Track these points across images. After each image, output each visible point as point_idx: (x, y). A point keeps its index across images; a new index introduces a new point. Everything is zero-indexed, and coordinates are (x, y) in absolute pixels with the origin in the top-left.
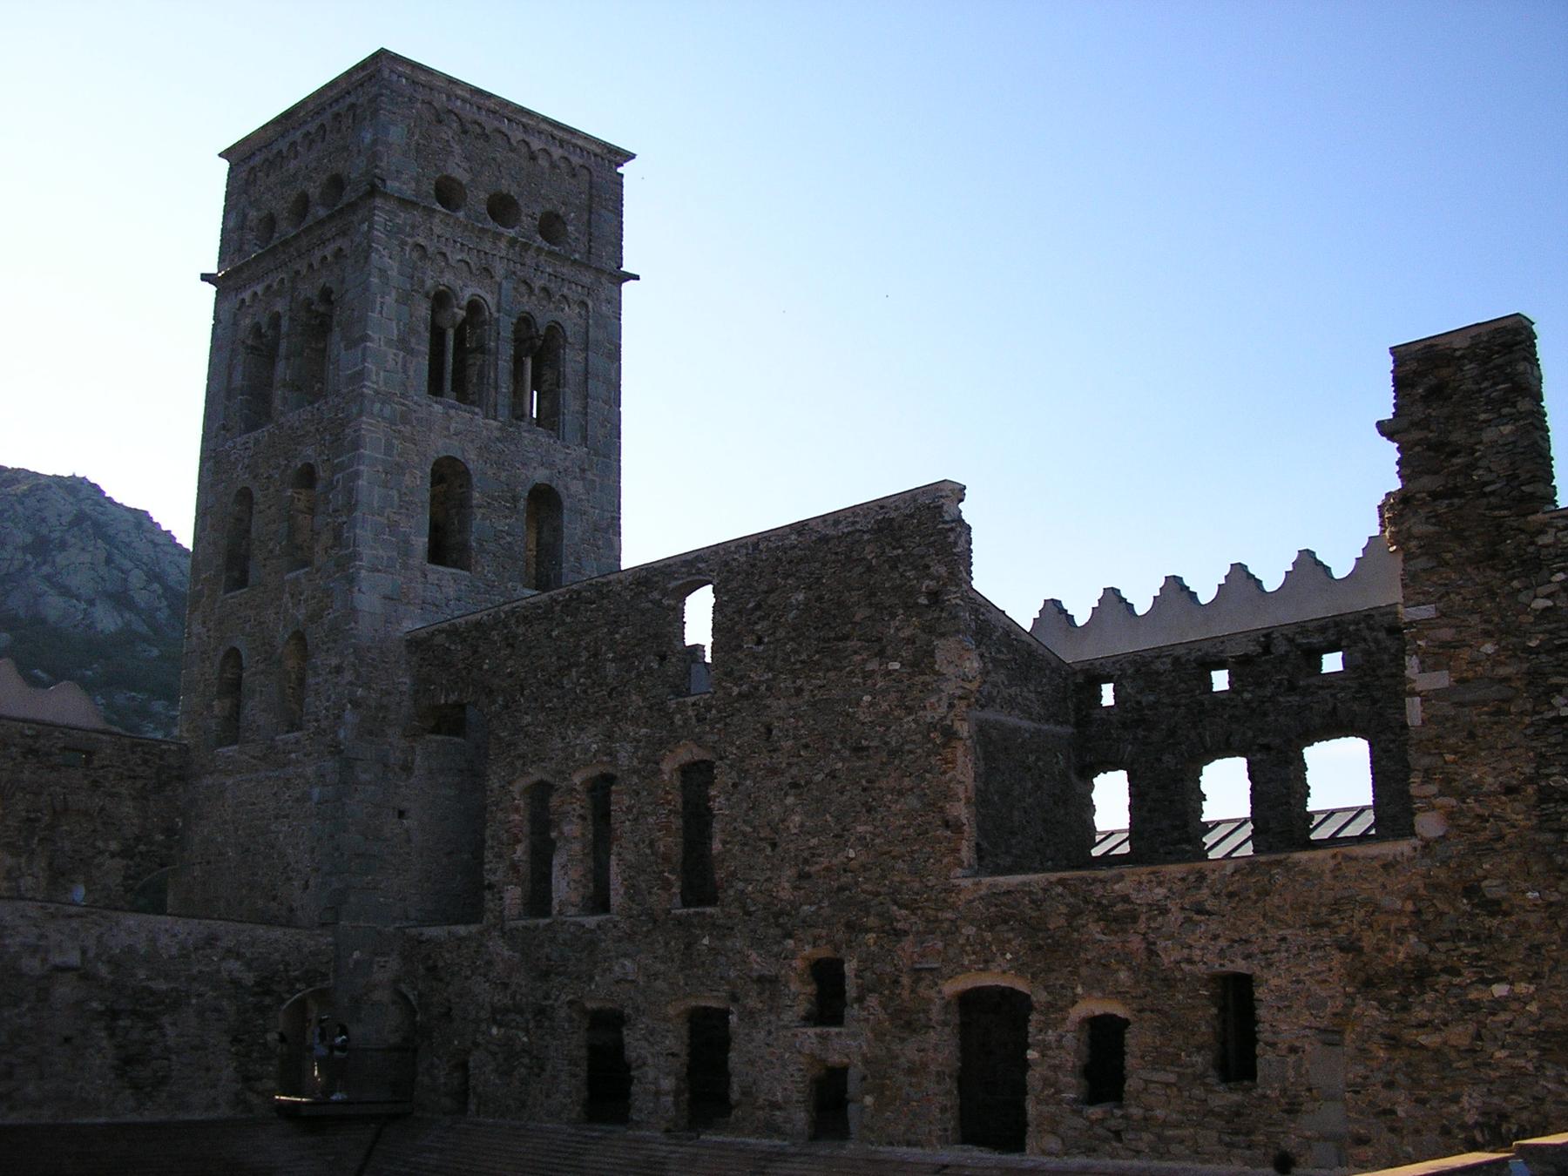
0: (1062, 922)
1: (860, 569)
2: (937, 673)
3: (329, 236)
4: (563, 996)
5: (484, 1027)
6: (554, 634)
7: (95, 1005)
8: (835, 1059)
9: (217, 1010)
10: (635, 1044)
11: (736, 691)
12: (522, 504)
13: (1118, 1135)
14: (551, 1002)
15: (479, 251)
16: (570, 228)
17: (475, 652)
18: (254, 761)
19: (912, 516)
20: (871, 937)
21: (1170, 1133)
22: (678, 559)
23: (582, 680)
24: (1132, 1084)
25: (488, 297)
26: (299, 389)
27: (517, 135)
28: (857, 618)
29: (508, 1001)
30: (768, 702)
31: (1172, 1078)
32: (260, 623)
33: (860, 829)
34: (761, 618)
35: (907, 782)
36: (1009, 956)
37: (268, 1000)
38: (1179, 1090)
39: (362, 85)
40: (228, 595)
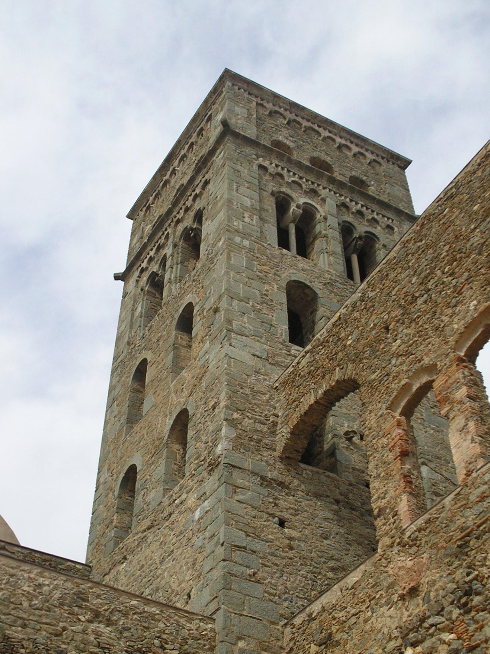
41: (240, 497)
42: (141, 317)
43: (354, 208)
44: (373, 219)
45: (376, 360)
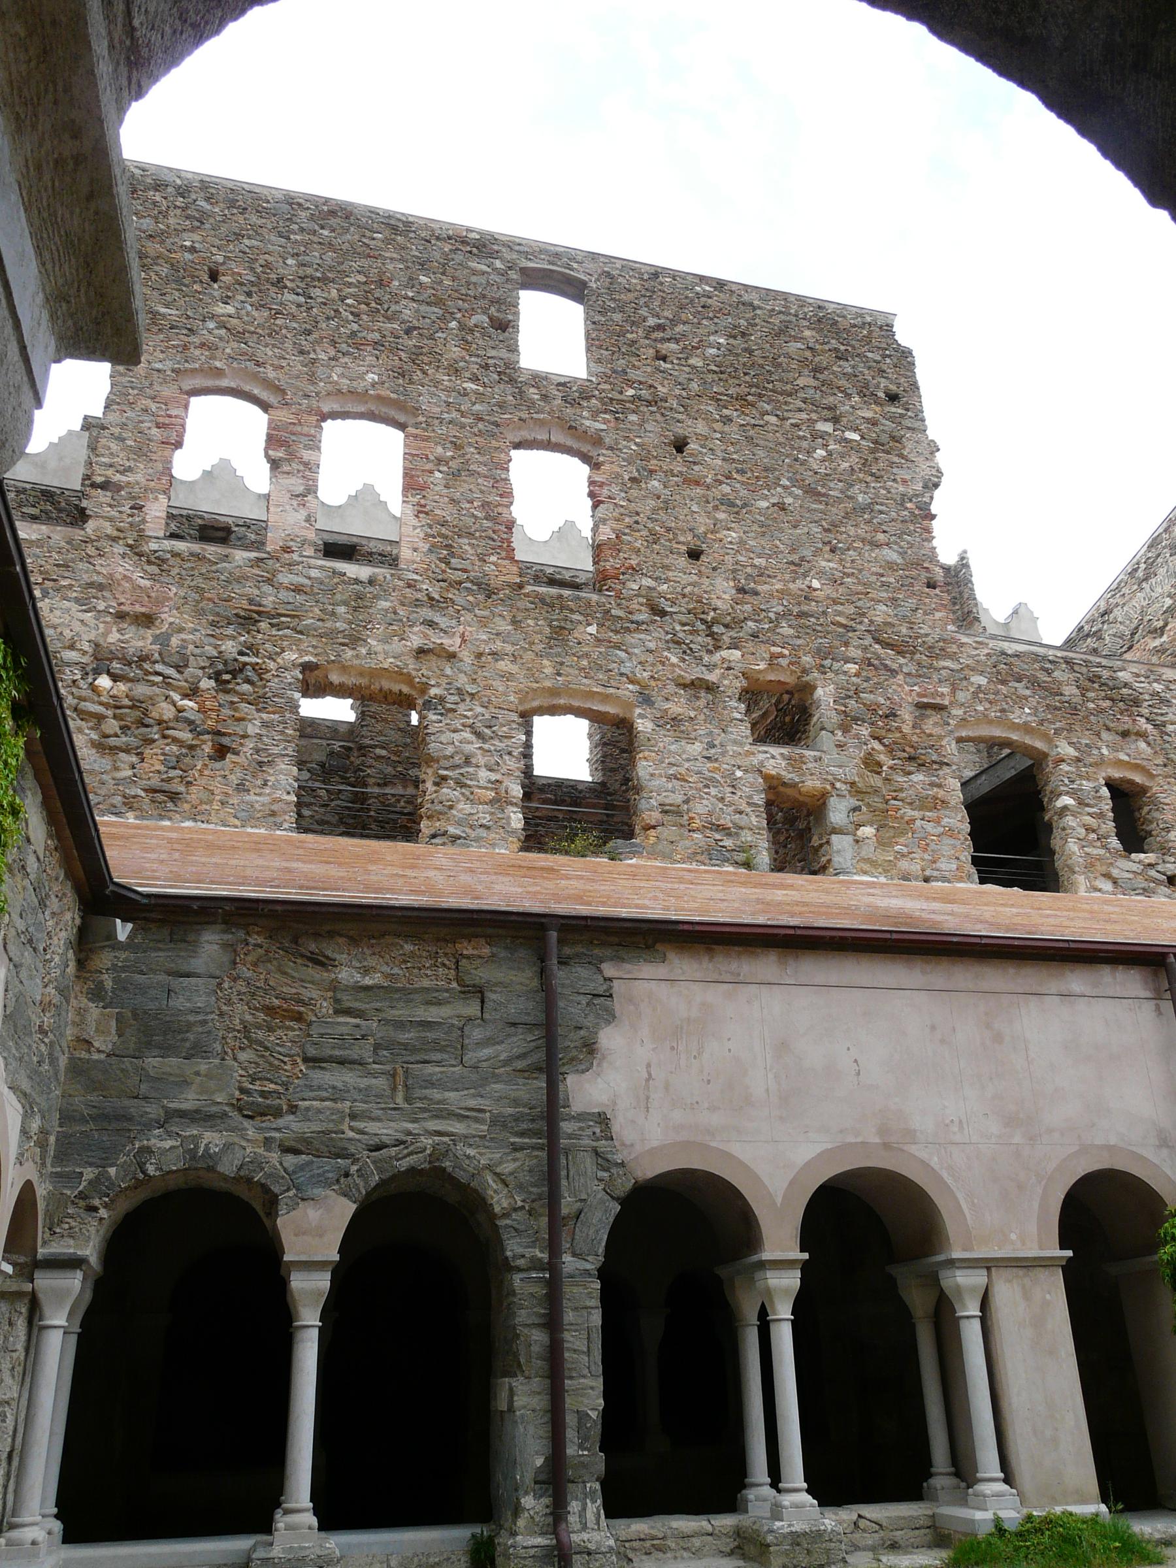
1: (799, 345)
2: (901, 456)
8: (812, 784)
11: (631, 392)
20: (852, 668)
23: (349, 301)
33: (824, 564)
34: (669, 340)
35: (881, 537)
36: (1027, 710)
45: (177, 293)
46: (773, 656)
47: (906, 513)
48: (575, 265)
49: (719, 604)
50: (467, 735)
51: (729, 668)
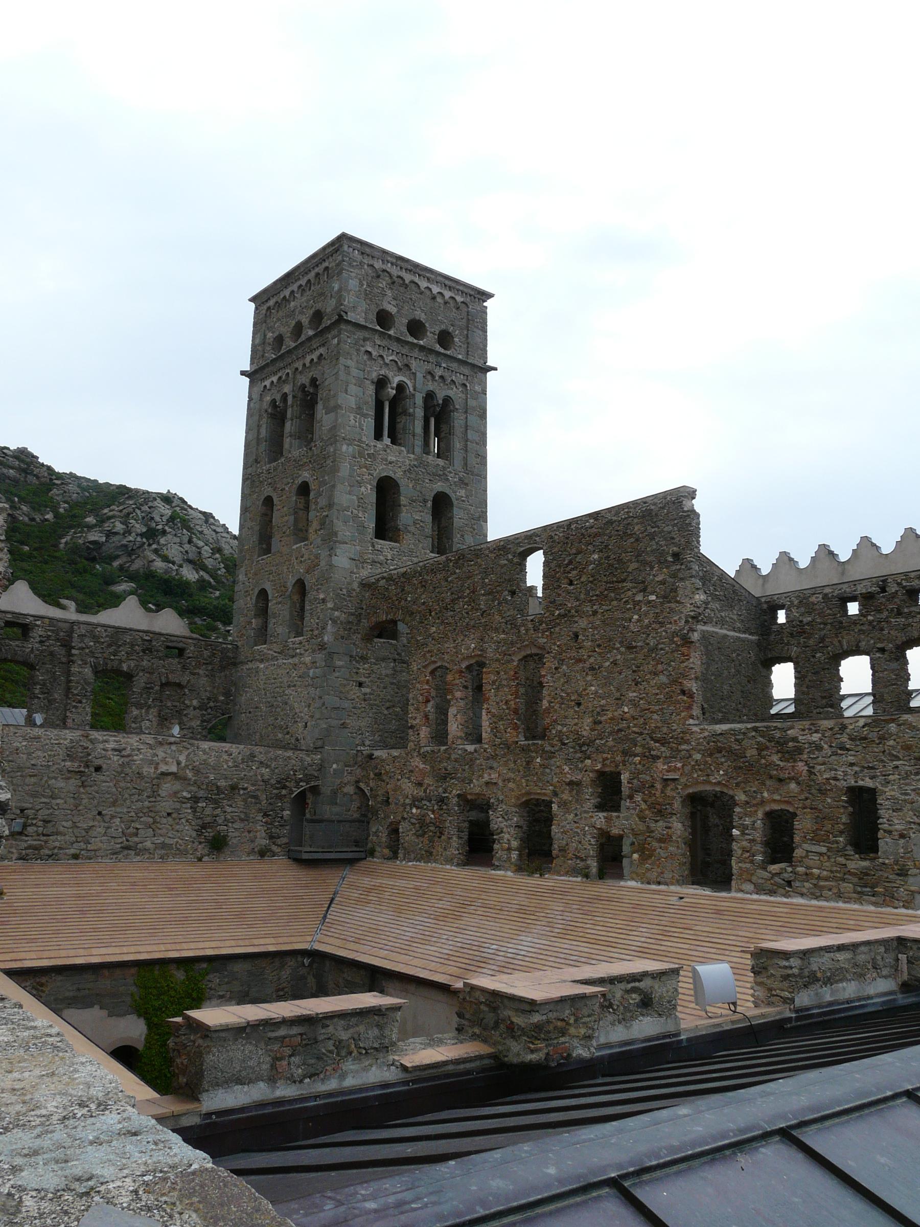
0: (755, 752)
1: (632, 540)
3: (315, 347)
4: (454, 792)
5: (408, 808)
6: (449, 579)
7: (185, 794)
8: (615, 831)
9: (256, 797)
10: (497, 821)
11: (557, 612)
12: (429, 504)
13: (789, 883)
14: (447, 795)
15: (402, 354)
16: (456, 340)
17: (403, 590)
18: (276, 654)
19: (663, 508)
21: (822, 883)
22: (523, 535)
23: (466, 606)
24: (798, 853)
25: (408, 382)
26: (299, 438)
27: (423, 284)
28: (630, 570)
29: (422, 794)
30: (576, 619)
31: (824, 850)
32: (279, 574)
33: (631, 695)
34: (573, 569)
35: (660, 667)
36: (721, 772)
37: (284, 792)
38: (829, 857)
39: (332, 256)
40: (260, 558)
41: (337, 674)
42: (266, 441)
43: (439, 372)
44: (452, 380)
46: (605, 759)
47: (674, 645)
48: (537, 539)
49: (584, 733)
50: (500, 819)
51: (586, 771)
